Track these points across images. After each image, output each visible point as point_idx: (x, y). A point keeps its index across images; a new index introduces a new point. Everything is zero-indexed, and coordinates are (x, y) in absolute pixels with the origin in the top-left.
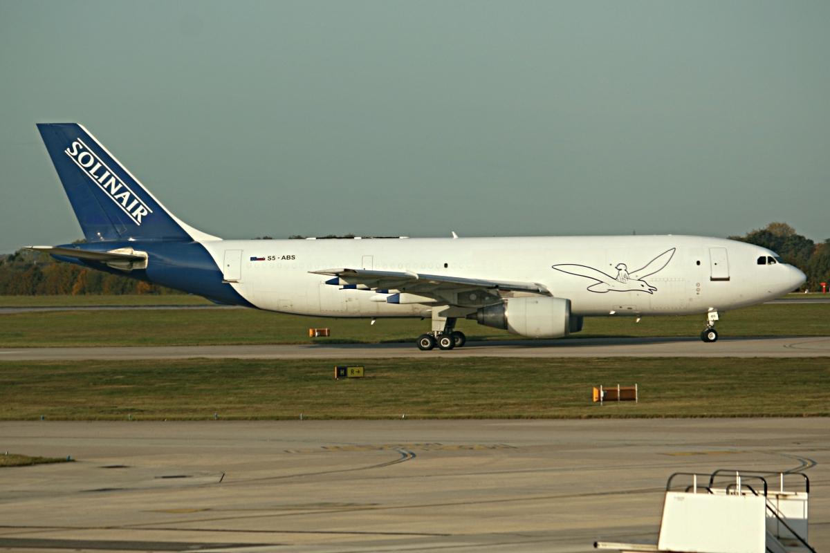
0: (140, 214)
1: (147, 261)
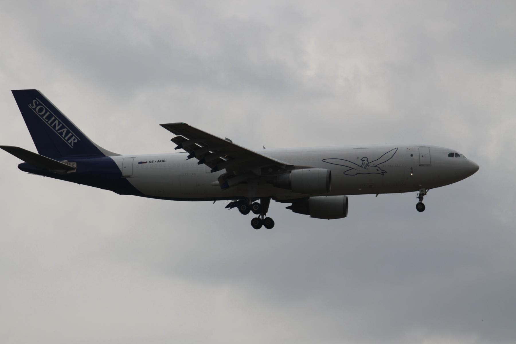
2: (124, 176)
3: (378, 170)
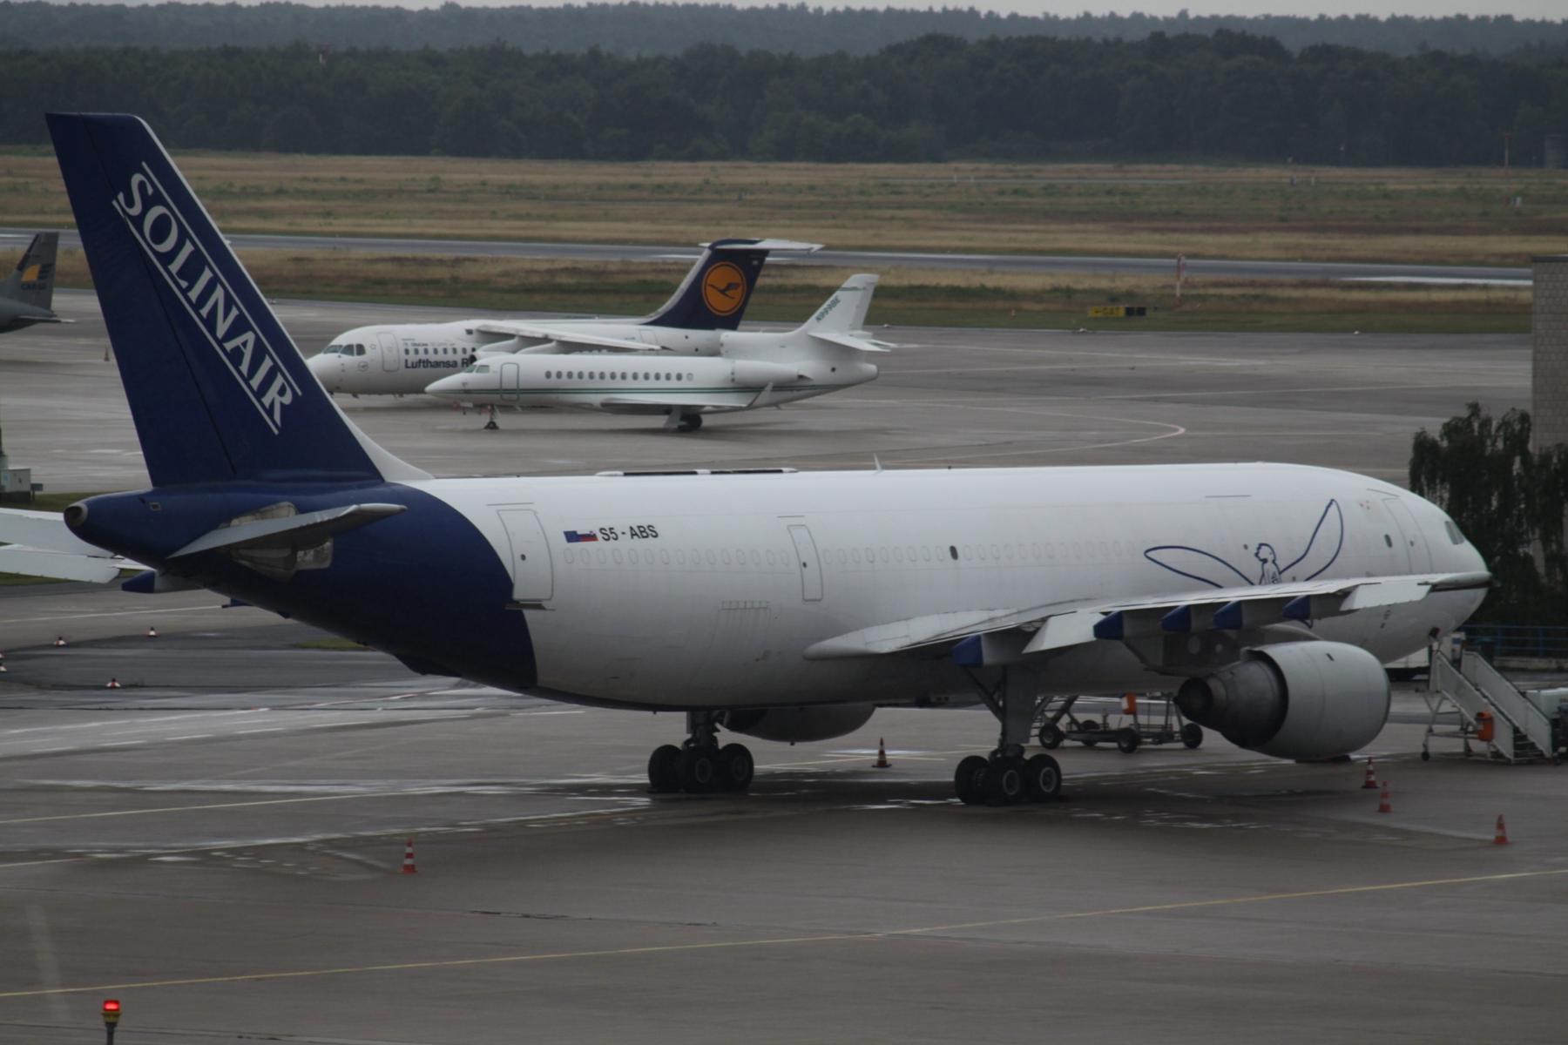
2: (517, 602)
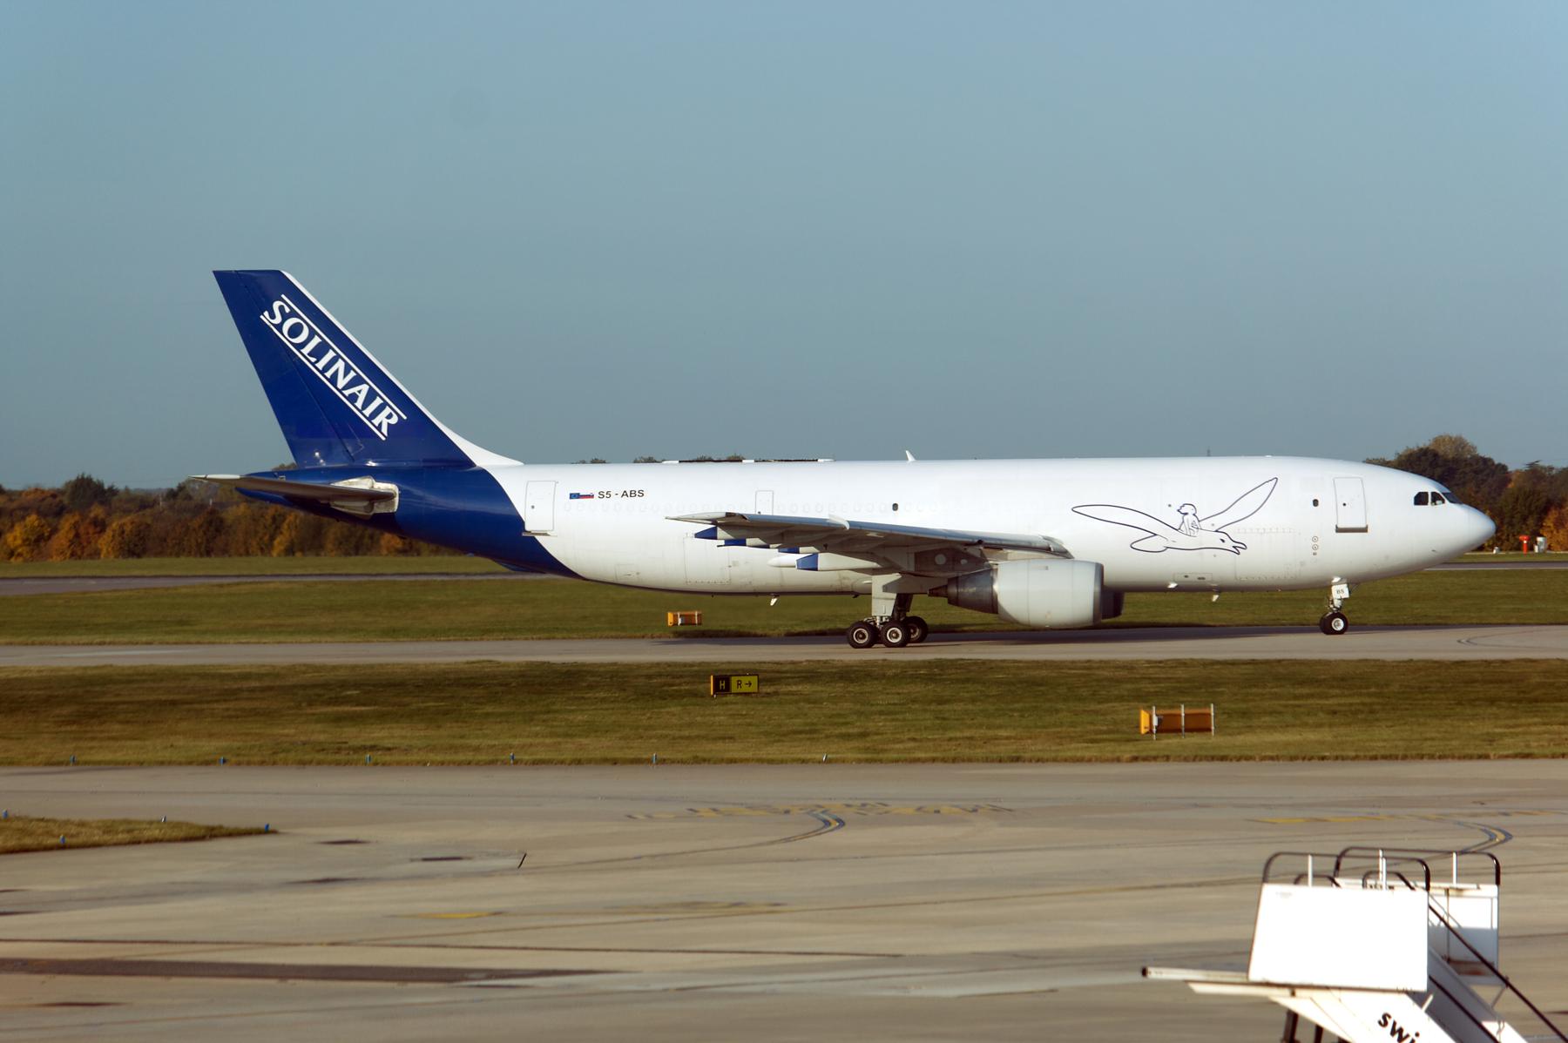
0: (384, 420)
1: (397, 499)
3: (1223, 541)
